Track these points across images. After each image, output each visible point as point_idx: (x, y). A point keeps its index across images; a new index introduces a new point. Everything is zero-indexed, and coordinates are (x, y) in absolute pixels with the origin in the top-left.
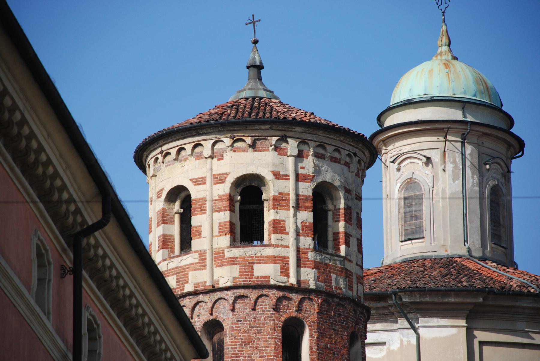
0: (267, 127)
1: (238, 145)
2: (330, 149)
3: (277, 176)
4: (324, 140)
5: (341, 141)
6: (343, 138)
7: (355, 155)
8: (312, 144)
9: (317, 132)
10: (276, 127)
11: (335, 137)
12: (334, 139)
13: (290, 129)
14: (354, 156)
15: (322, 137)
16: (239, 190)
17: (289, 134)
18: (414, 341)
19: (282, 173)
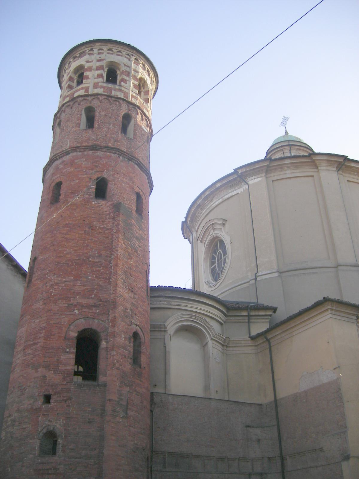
0: (84, 47)
1: (76, 59)
2: (115, 51)
3: (87, 62)
4: (111, 47)
5: (121, 48)
6: (122, 47)
7: (132, 55)
8: (105, 49)
9: (107, 44)
10: (87, 46)
11: (117, 46)
12: (117, 47)
13: (94, 45)
14: (131, 56)
15: (110, 46)
16: (77, 75)
17: (93, 47)
18: (247, 187)
19: (90, 61)
